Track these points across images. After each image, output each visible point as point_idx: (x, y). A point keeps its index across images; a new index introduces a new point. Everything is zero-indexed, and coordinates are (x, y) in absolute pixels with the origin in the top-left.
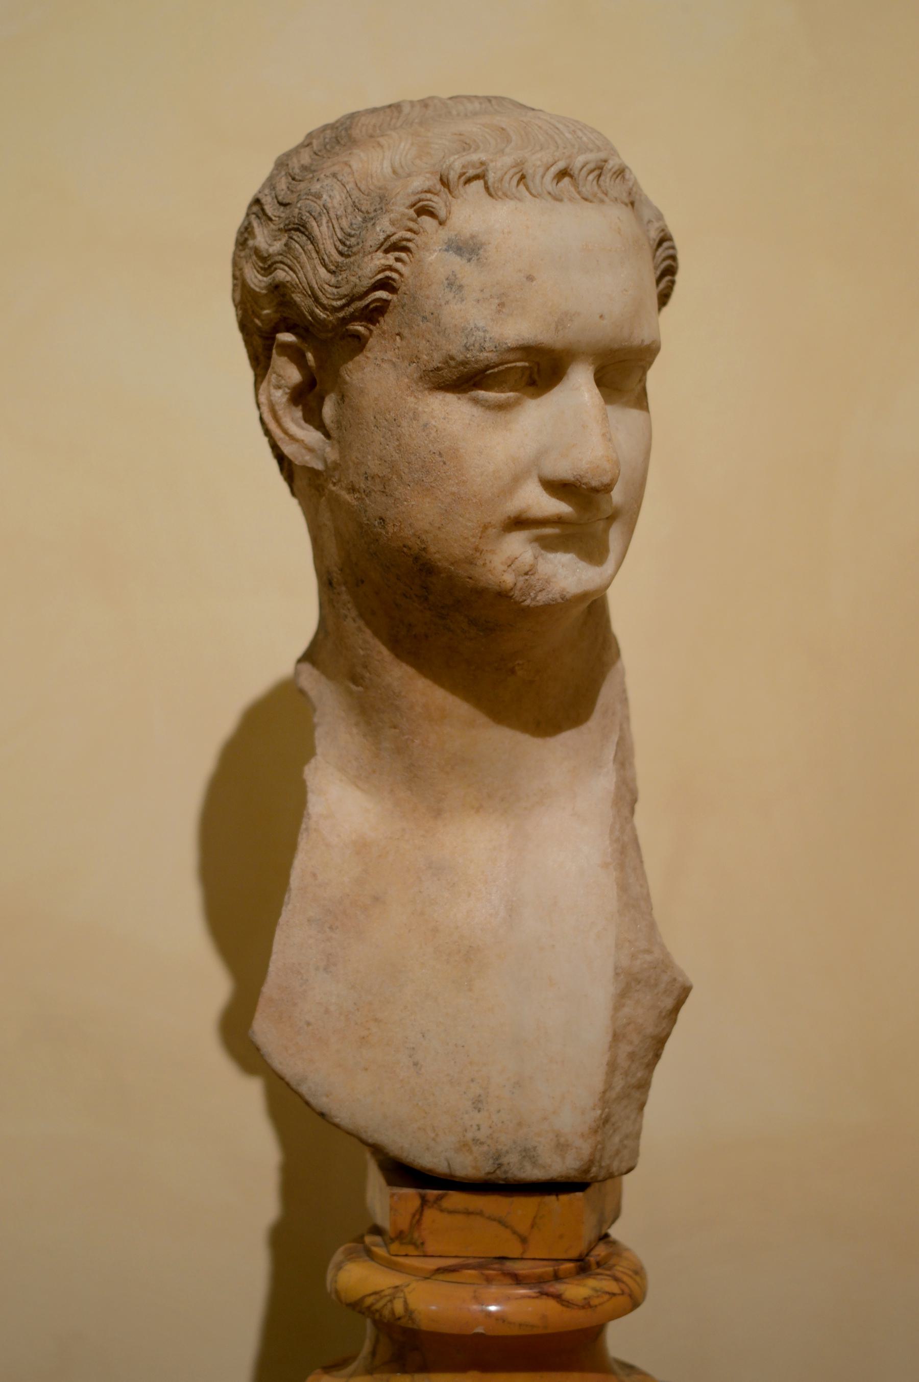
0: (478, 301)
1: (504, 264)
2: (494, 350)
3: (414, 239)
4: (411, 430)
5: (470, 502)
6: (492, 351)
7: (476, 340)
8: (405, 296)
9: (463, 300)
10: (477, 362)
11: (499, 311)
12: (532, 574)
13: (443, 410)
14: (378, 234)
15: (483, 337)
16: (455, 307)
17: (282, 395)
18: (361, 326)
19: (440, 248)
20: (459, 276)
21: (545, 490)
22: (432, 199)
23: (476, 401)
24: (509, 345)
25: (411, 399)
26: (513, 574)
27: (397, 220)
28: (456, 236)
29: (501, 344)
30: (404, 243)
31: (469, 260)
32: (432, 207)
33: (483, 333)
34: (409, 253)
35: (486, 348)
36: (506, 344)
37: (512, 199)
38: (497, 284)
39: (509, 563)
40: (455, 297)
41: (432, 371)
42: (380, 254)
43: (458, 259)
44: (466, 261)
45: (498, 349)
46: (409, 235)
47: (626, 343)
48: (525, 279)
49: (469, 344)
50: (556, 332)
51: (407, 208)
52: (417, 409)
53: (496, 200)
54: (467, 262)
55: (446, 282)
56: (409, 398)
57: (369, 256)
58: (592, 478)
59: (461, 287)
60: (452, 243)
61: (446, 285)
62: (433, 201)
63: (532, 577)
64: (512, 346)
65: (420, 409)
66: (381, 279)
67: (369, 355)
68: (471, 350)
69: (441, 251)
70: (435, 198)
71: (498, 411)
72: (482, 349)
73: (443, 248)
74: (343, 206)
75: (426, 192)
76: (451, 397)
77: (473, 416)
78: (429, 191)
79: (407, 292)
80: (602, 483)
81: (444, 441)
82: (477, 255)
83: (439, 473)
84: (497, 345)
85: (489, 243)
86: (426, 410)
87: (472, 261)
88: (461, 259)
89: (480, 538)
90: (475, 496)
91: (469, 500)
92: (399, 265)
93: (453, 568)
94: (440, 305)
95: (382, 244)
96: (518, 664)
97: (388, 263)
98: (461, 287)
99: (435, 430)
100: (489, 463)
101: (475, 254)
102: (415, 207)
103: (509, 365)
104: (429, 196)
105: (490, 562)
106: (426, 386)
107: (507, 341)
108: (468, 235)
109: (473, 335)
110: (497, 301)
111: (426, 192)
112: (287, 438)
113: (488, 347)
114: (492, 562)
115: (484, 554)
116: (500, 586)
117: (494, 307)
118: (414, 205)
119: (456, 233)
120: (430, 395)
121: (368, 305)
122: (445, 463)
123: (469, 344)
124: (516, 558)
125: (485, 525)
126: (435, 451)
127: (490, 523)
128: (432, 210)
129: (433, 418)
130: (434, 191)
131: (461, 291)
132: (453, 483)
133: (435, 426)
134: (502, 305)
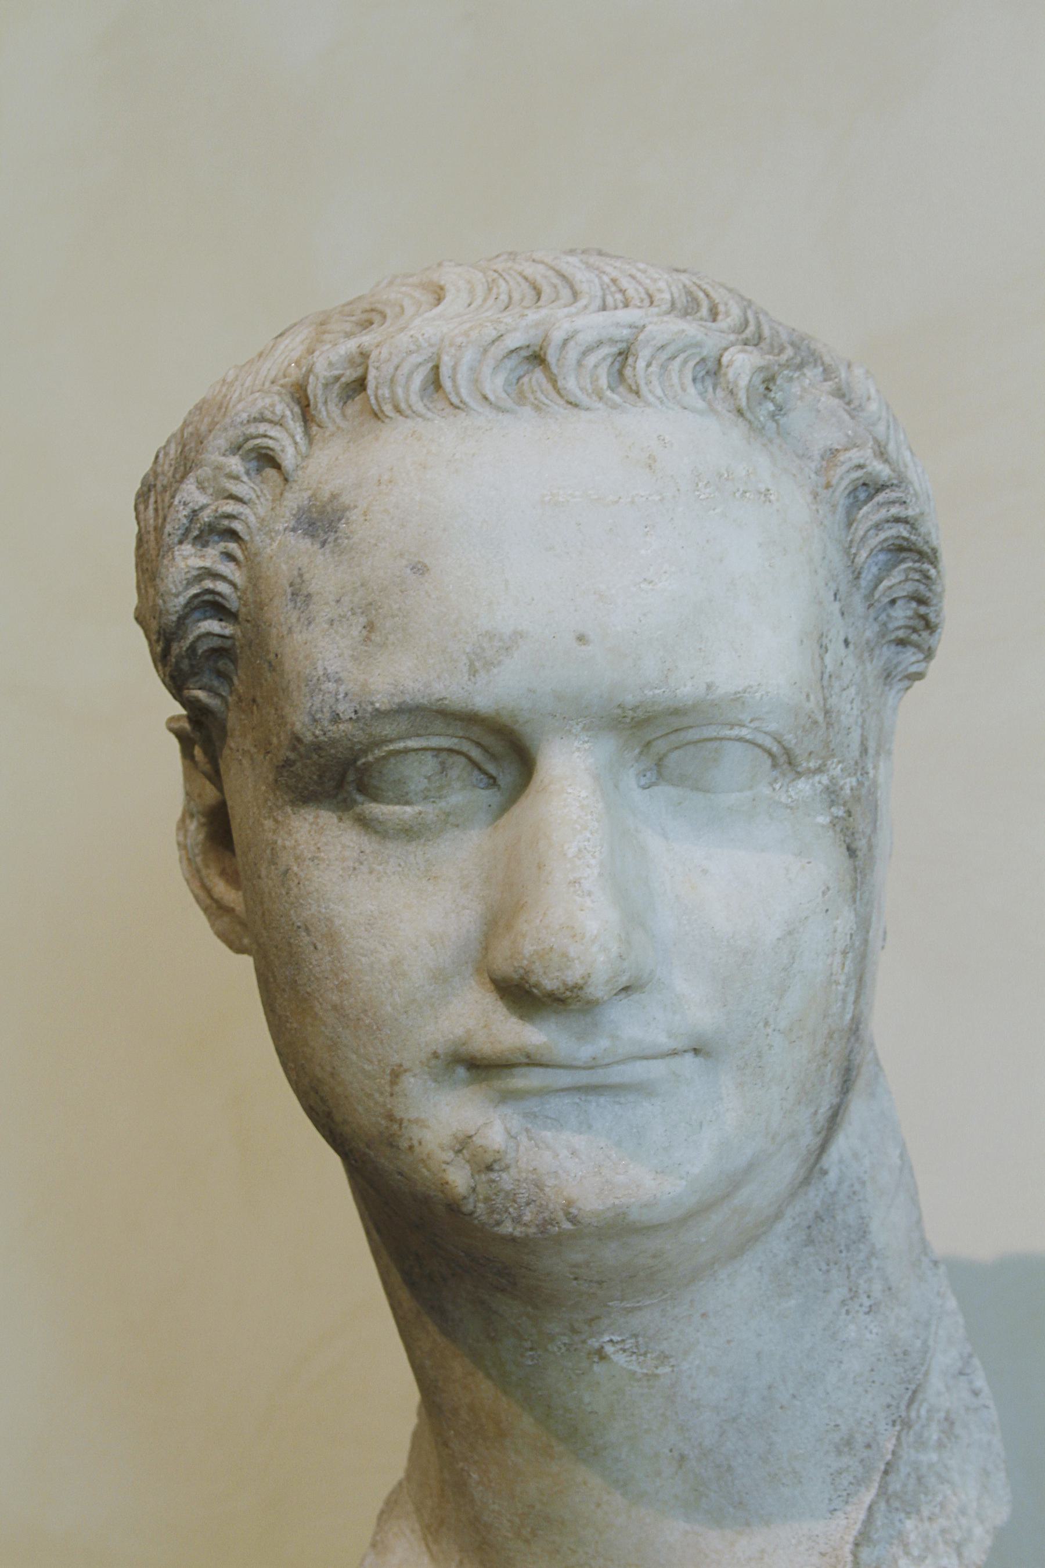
0: (331, 622)
1: (376, 545)
2: (354, 716)
3: (241, 514)
4: (270, 882)
5: (361, 1023)
6: (351, 719)
7: (323, 700)
8: (249, 625)
9: (310, 623)
10: (333, 742)
11: (367, 639)
12: (502, 1170)
13: (313, 842)
14: (177, 509)
15: (334, 692)
16: (299, 637)
17: (197, 829)
18: (200, 689)
19: (286, 525)
20: (307, 576)
21: (501, 998)
22: (269, 433)
23: (365, 823)
24: (377, 705)
25: (268, 824)
26: (468, 1167)
27: (208, 480)
28: (310, 498)
29: (364, 705)
30: (226, 522)
31: (323, 544)
32: (268, 448)
33: (335, 685)
34: (240, 542)
35: (341, 715)
36: (372, 703)
37: (407, 417)
38: (362, 585)
39: (458, 1147)
40: (299, 619)
41: (283, 766)
42: (187, 548)
43: (308, 541)
44: (319, 546)
45: (359, 715)
46: (230, 507)
47: (657, 691)
48: (409, 571)
49: (314, 708)
50: (470, 675)
51: (224, 455)
52: (276, 842)
53: (383, 422)
54: (320, 548)
55: (289, 590)
56: (266, 822)
57: (170, 553)
58: (545, 973)
59: (309, 596)
60: (303, 514)
61: (289, 597)
62: (271, 438)
63: (504, 1175)
64: (383, 708)
65: (280, 842)
66: (196, 596)
67: (233, 745)
68: (320, 719)
69: (286, 532)
70: (273, 432)
71: (409, 841)
72: (336, 719)
73: (291, 526)
74: (172, 468)
75: (255, 420)
76: (327, 817)
77: (362, 852)
78: (262, 419)
79: (249, 618)
80: (565, 984)
81: (310, 904)
82: (336, 532)
83: (311, 967)
84: (358, 707)
85: (356, 507)
86: (287, 843)
87: (327, 546)
88: (312, 544)
89: (392, 1095)
90: (366, 1011)
91: (358, 1019)
92: (227, 568)
93: (372, 1153)
94: (283, 636)
95: (188, 530)
96: (611, 1341)
97: (208, 564)
98: (309, 596)
99: (296, 881)
100: (384, 945)
101: (332, 531)
102: (240, 452)
103: (391, 747)
104: (263, 428)
105: (420, 1143)
106: (286, 798)
107: (374, 699)
108: (327, 495)
109: (320, 690)
110: (363, 620)
111: (255, 420)
112: (214, 906)
113: (343, 713)
114: (423, 1143)
115: (406, 1127)
116: (442, 1192)
117: (355, 632)
118: (239, 448)
119: (310, 493)
120: (295, 814)
121: (192, 648)
122: (316, 948)
123: (314, 708)
124: (470, 1137)
125: (393, 1070)
126: (299, 924)
127: (401, 1065)
128: (271, 453)
129: (297, 858)
130: (268, 415)
131: (308, 605)
132: (331, 985)
133: (296, 874)
134: (370, 627)
